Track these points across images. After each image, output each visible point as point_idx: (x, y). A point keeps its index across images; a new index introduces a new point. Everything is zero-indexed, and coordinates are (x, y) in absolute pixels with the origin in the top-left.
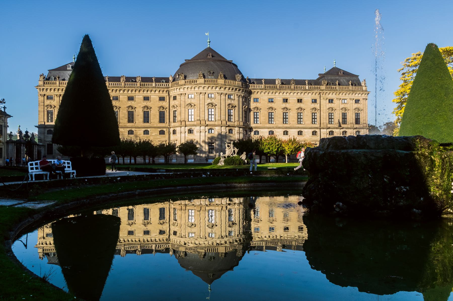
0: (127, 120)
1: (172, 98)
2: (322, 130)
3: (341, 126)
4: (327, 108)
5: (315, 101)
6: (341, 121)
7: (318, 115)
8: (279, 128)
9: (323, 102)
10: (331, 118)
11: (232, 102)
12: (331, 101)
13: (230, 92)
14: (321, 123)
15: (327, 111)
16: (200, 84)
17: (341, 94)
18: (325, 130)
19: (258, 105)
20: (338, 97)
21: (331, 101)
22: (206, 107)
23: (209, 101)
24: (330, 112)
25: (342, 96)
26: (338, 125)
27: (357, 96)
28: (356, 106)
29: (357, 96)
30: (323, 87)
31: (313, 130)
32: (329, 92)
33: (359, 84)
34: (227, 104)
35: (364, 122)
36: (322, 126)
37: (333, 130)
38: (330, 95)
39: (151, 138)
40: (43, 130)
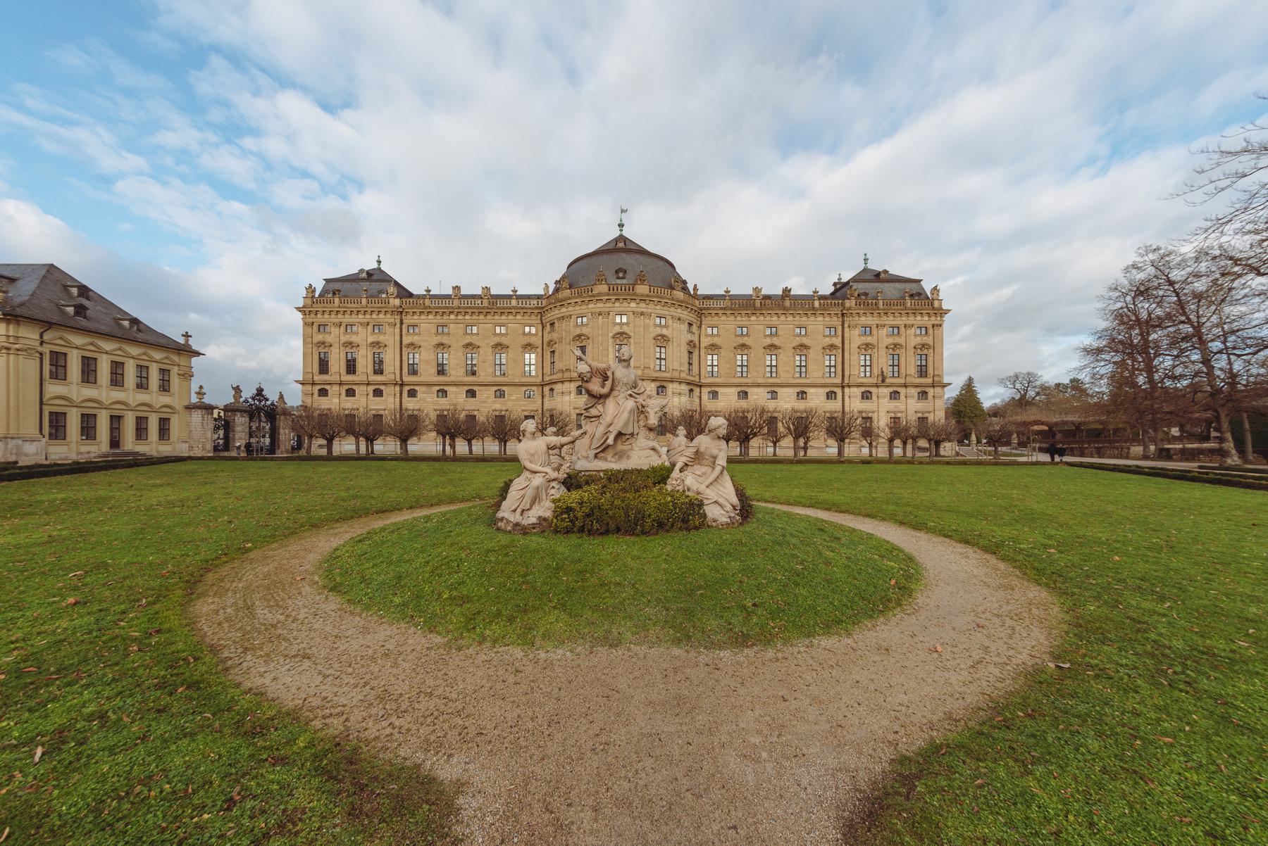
0: (463, 370)
1: (548, 328)
2: (847, 390)
8: (759, 386)
11: (664, 331)
13: (658, 309)
16: (600, 294)
18: (854, 390)
19: (716, 341)
22: (611, 340)
23: (618, 329)
30: (850, 303)
31: (828, 390)
34: (653, 335)
36: (846, 381)
39: (510, 405)
40: (309, 387)
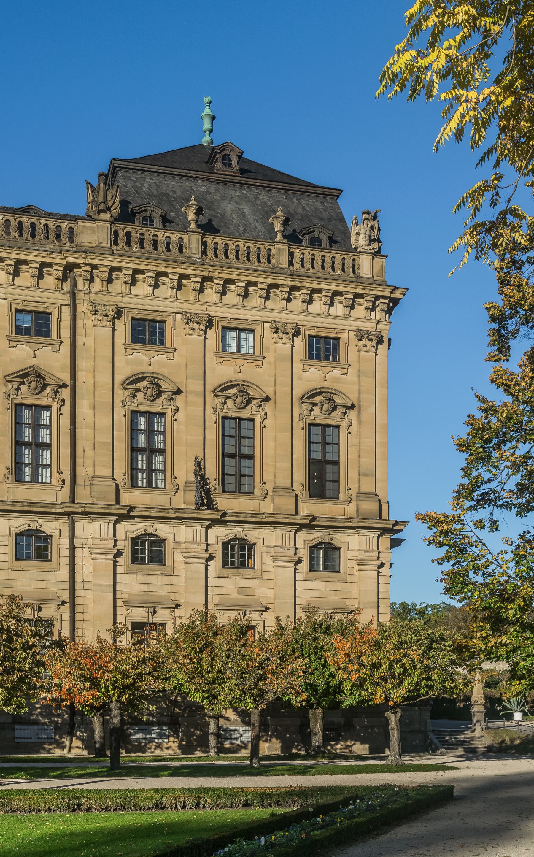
3: (211, 506)
4: (119, 378)
5: (35, 325)
6: (212, 471)
7: (56, 425)
9: (95, 335)
10: (144, 449)
12: (148, 331)
14: (80, 480)
15: (121, 395)
17: (211, 294)
20: (192, 308)
21: (148, 331)
24: (141, 403)
25: (228, 308)
26: (192, 497)
27: (318, 316)
28: (313, 376)
29: (318, 316)
32: (129, 265)
33: (338, 239)
35: (367, 486)
37: (164, 530)
38: (142, 288)
